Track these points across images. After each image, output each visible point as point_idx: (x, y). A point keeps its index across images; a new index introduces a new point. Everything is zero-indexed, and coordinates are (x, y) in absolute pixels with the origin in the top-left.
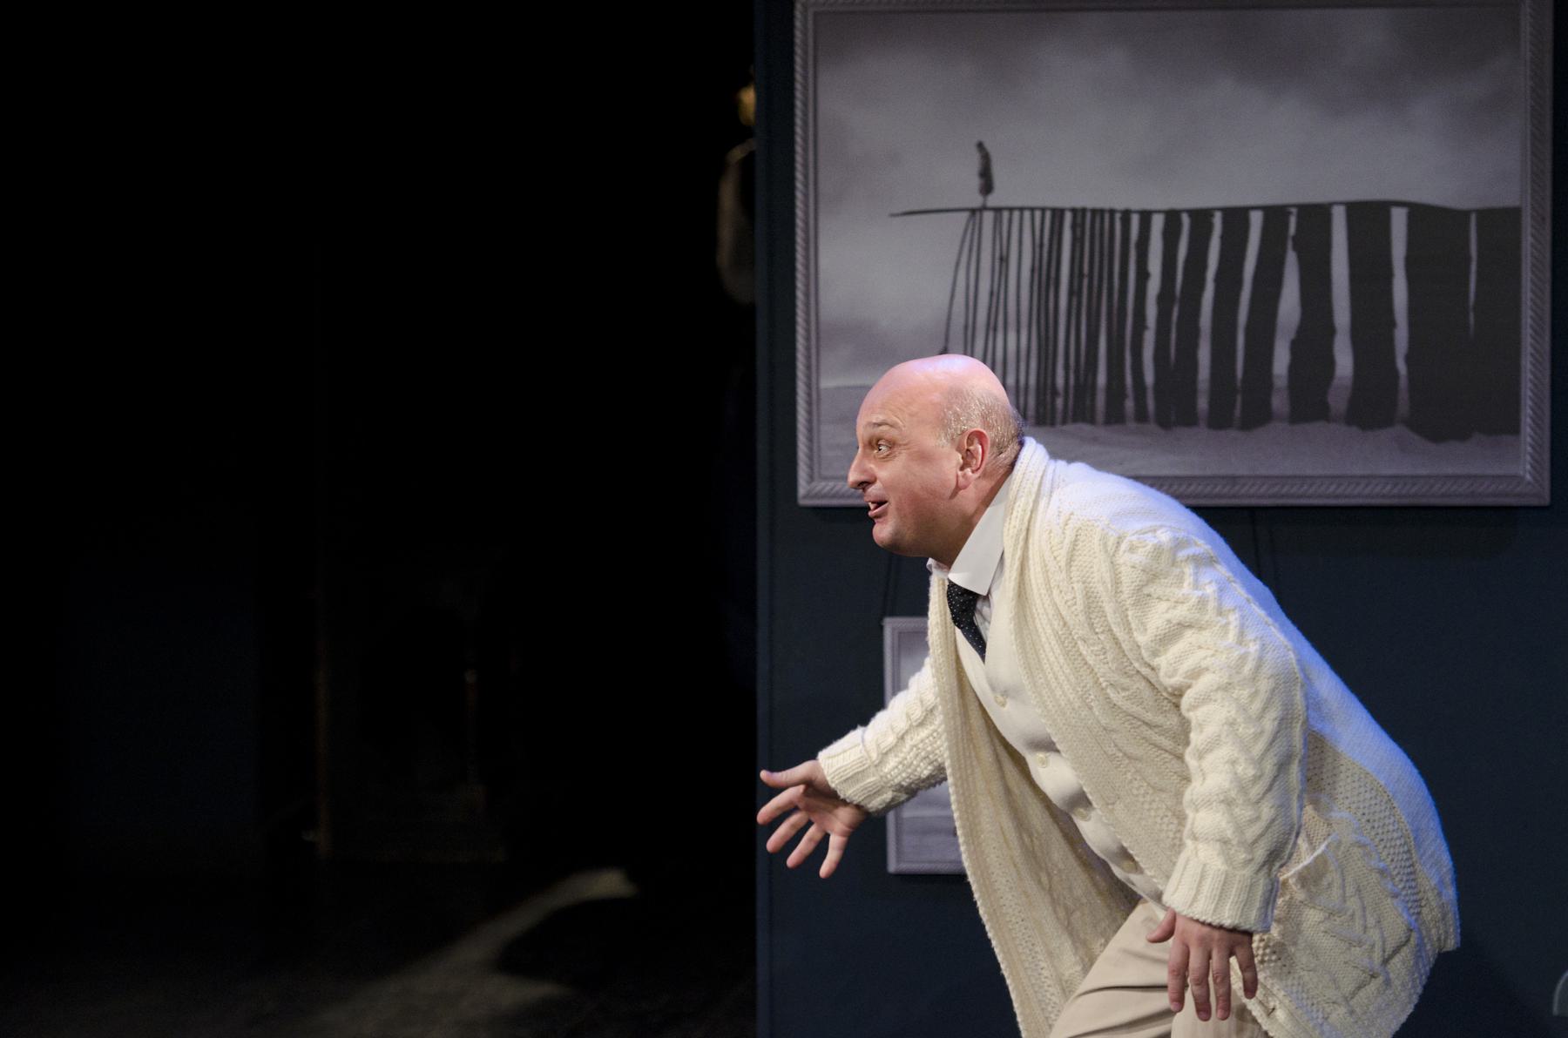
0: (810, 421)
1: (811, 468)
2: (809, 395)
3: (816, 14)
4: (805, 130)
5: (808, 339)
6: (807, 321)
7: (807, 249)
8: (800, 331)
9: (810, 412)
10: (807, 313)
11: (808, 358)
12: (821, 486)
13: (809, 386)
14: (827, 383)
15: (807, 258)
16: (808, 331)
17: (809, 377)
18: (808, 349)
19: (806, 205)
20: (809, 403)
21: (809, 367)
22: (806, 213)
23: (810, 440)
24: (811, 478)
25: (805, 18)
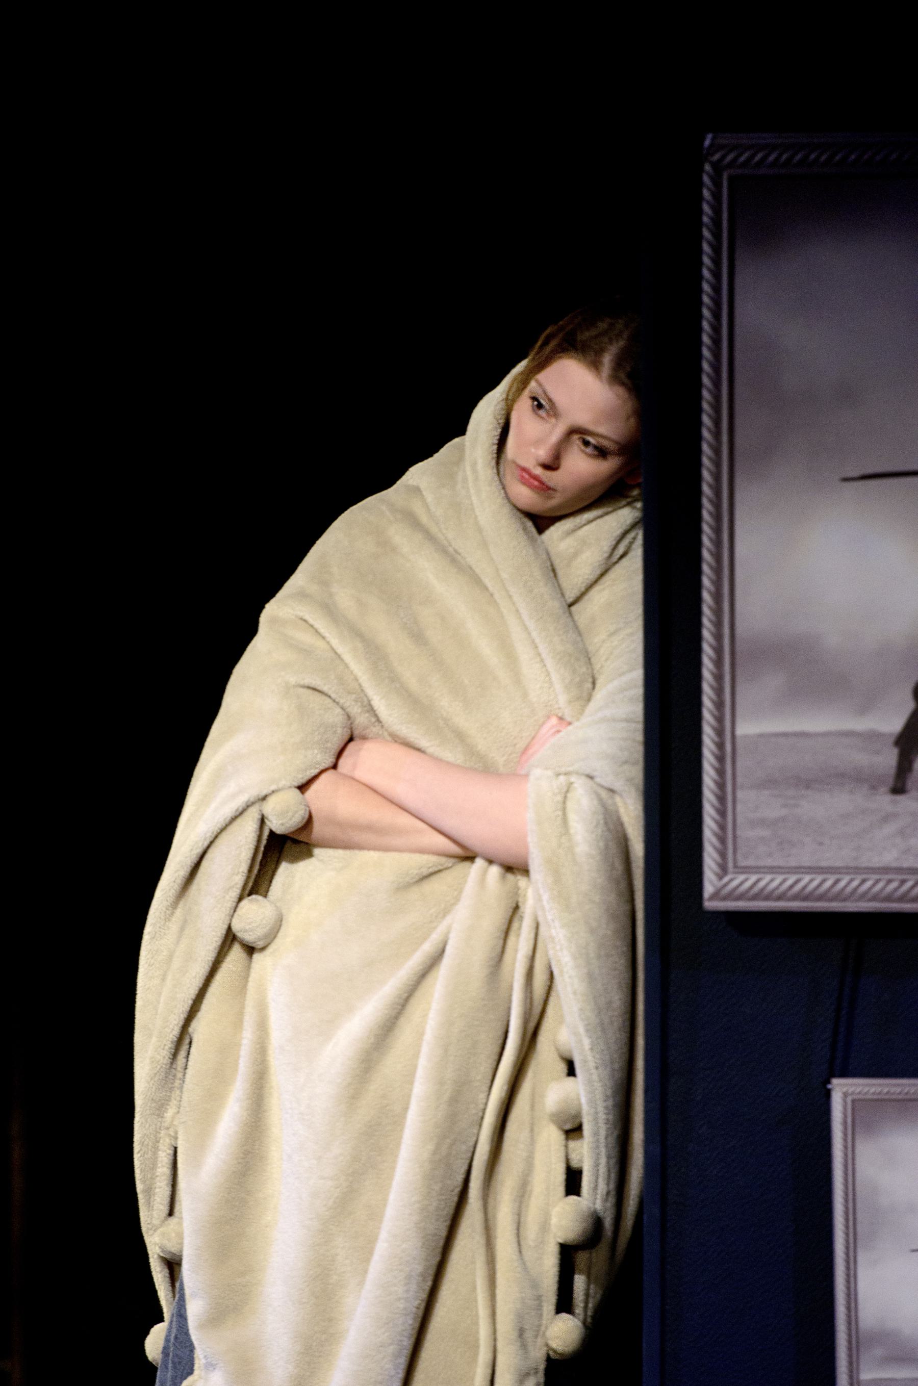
0: (721, 785)
1: (723, 854)
2: (720, 746)
3: (731, 179)
4: (717, 354)
5: (718, 662)
6: (718, 637)
7: (718, 530)
8: (707, 650)
9: (721, 772)
10: (718, 624)
11: (719, 691)
12: (739, 881)
13: (720, 732)
14: (746, 728)
15: (718, 543)
16: (719, 650)
17: (720, 719)
18: (719, 678)
19: (717, 464)
20: (721, 759)
21: (719, 705)
22: (717, 477)
23: (722, 813)
24: (723, 869)
25: (717, 183)
